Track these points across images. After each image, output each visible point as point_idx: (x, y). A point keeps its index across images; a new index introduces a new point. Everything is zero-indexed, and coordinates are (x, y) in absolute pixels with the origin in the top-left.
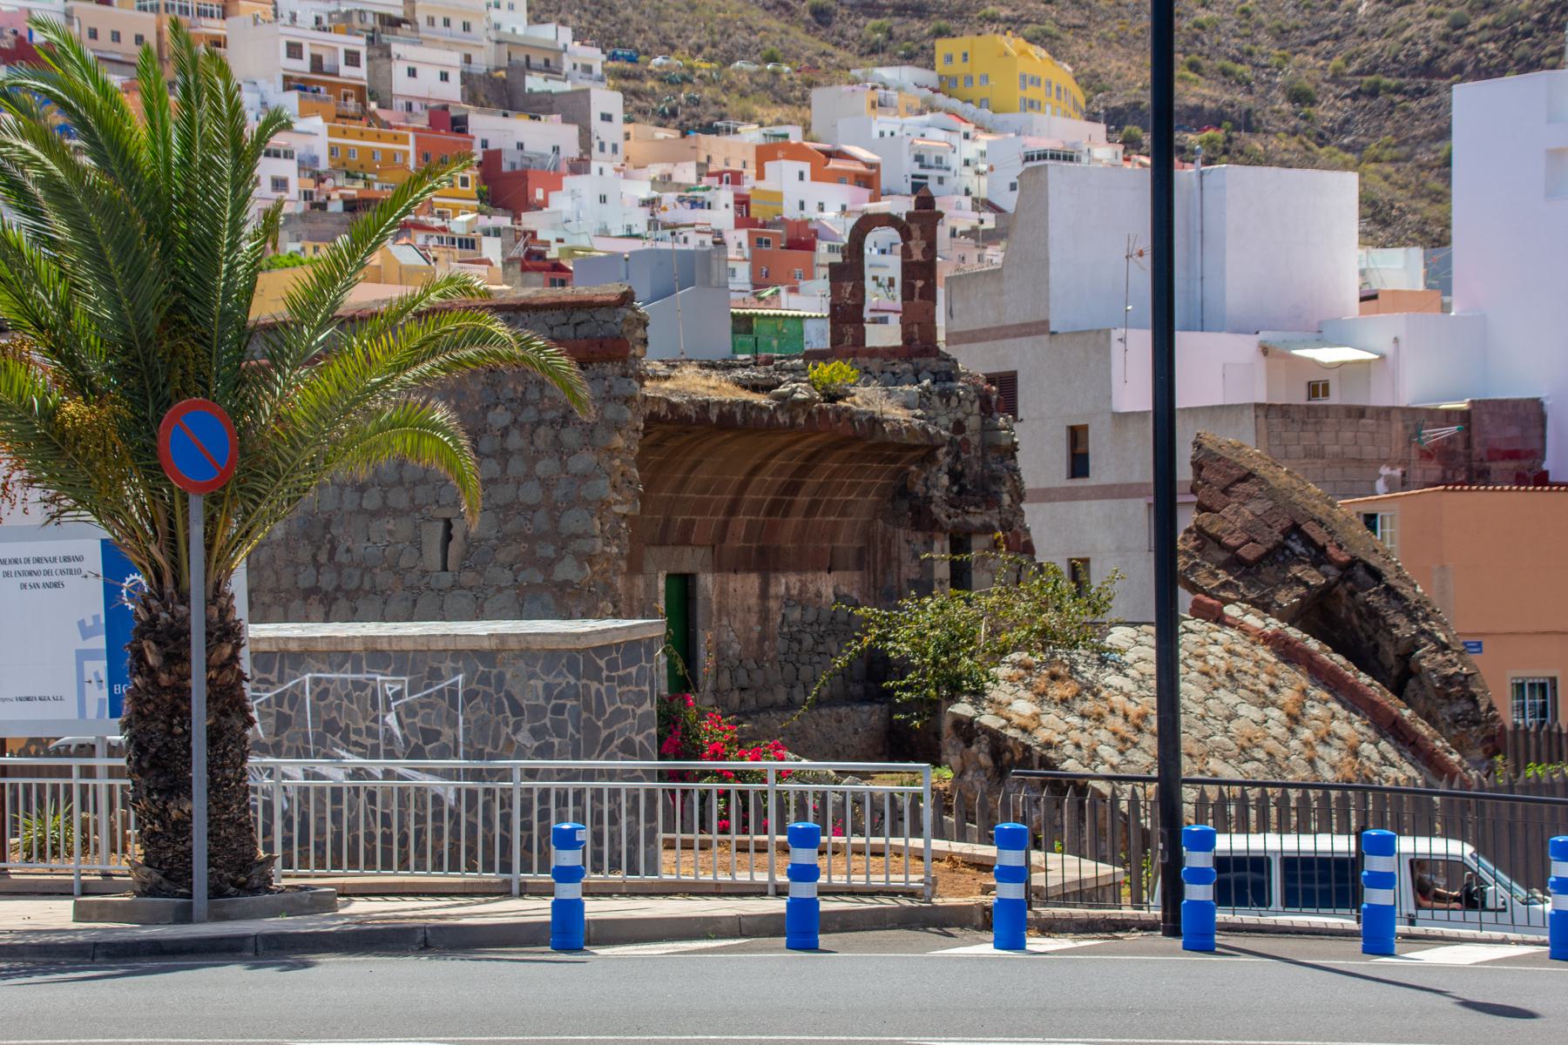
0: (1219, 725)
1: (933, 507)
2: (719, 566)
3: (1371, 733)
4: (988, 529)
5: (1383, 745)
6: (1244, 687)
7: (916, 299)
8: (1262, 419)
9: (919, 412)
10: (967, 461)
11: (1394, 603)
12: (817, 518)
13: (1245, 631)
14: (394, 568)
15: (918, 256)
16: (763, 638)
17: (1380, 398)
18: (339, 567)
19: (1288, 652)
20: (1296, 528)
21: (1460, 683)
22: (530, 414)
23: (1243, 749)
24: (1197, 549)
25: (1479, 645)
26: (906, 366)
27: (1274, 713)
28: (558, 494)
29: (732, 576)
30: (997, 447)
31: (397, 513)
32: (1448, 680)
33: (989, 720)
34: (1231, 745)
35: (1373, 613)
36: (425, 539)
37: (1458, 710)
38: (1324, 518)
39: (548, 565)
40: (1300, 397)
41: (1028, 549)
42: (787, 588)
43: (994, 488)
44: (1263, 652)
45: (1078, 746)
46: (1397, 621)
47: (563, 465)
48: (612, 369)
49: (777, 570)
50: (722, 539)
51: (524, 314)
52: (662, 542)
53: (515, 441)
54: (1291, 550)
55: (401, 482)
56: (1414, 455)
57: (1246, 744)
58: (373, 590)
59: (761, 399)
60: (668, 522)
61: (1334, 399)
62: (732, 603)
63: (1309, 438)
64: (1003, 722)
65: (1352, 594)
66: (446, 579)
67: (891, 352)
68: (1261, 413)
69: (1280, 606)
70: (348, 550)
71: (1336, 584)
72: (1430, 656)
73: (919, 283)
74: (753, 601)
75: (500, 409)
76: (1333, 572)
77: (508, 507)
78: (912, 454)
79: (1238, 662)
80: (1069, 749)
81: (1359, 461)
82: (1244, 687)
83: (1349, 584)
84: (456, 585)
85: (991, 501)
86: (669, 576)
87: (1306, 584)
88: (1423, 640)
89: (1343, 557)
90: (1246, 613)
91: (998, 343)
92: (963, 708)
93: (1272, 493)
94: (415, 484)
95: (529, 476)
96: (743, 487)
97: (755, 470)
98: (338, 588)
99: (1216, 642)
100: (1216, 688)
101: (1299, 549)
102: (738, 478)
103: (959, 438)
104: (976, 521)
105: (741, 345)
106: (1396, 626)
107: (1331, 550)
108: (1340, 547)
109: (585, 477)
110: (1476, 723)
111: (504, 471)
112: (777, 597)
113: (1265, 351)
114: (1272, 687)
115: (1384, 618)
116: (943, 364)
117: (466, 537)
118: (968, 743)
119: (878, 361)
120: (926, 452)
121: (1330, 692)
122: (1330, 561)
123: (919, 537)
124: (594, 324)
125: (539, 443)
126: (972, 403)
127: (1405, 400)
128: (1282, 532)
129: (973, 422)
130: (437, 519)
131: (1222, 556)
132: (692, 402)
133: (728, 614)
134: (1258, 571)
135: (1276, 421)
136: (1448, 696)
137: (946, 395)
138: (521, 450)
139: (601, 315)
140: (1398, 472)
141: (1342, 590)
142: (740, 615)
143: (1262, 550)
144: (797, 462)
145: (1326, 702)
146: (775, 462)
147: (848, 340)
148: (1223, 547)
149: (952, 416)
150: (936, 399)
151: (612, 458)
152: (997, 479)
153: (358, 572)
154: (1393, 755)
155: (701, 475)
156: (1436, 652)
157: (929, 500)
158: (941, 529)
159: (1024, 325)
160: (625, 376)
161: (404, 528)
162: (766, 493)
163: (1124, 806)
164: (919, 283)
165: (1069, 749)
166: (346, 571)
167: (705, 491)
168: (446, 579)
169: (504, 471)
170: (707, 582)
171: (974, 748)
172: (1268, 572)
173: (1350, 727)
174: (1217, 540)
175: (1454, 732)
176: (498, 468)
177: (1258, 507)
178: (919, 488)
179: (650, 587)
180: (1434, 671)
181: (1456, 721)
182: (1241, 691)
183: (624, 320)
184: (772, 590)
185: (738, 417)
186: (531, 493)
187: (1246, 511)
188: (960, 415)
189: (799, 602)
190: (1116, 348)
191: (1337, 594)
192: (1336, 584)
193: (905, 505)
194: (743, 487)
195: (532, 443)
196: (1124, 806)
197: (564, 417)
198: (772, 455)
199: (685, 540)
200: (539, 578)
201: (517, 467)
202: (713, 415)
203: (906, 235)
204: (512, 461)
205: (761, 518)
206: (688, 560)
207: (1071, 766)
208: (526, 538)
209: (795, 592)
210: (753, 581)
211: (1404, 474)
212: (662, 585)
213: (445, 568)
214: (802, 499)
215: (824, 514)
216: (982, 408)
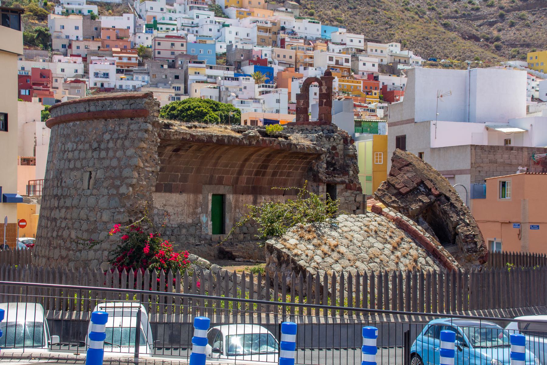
0: (365, 250)
1: (320, 175)
2: (236, 191)
3: (424, 254)
4: (342, 182)
5: (428, 259)
6: (380, 237)
7: (323, 106)
8: (473, 150)
9: (315, 142)
10: (338, 160)
11: (453, 209)
12: (277, 177)
13: (387, 216)
14: (76, 189)
15: (324, 91)
17: (526, 144)
18: (62, 187)
19: (400, 225)
20: (422, 182)
21: (471, 238)
22: (116, 136)
23: (371, 258)
24: (386, 189)
25: (538, 226)
26: (319, 128)
27: (388, 246)
28: (122, 163)
29: (241, 196)
30: (349, 156)
31: (78, 169)
32: (467, 236)
33: (279, 246)
34: (367, 256)
35: (445, 213)
36: (84, 178)
37: (469, 247)
38: (433, 179)
39: (118, 188)
40: (502, 144)
41: (360, 189)
43: (347, 169)
44: (392, 225)
45: (307, 256)
46: (453, 215)
47: (125, 153)
48: (141, 120)
49: (261, 194)
50: (237, 183)
51: (115, 101)
52: (210, 183)
53: (111, 145)
54: (420, 190)
55: (79, 159)
56: (531, 163)
57: (373, 257)
58: (70, 196)
59: (238, 135)
60: (212, 177)
61: (512, 144)
62: (240, 205)
63: (491, 156)
64: (283, 246)
65: (439, 205)
66: (89, 192)
67: (315, 123)
68: (473, 148)
69: (412, 209)
70: (65, 182)
71: (434, 202)
72: (461, 228)
73: (325, 100)
76: (433, 197)
77: (108, 167)
78: (311, 157)
79: (381, 228)
80: (304, 257)
81: (510, 165)
82: (380, 237)
83: (438, 202)
84: (91, 194)
85: (346, 173)
86: (214, 195)
87: (422, 202)
88: (461, 222)
89: (437, 193)
90: (390, 211)
91: (401, 126)
92: (271, 242)
93: (416, 170)
94: (83, 159)
95: (114, 157)
96: (243, 166)
97: (246, 160)
98: (62, 195)
99: (376, 221)
100: (368, 237)
101: (422, 189)
102: (240, 163)
103: (334, 152)
104: (339, 180)
105: (358, 130)
106: (452, 217)
107: (433, 190)
108: (436, 189)
109: (130, 157)
110: (476, 252)
111: (107, 155)
113: (487, 129)
114: (391, 237)
115: (448, 214)
116: (331, 127)
117: (95, 178)
118: (271, 253)
119: (310, 126)
120: (318, 156)
121: (412, 239)
122: (432, 194)
123: (315, 184)
124: (136, 104)
125: (118, 145)
126: (340, 140)
127: (534, 145)
128: (417, 184)
129: (340, 147)
130: (87, 171)
131: (395, 192)
132: (205, 135)
133: (239, 208)
134: (407, 197)
135: (479, 151)
136: (466, 242)
137: (328, 138)
138: (112, 148)
139: (138, 101)
140: (525, 169)
141: (436, 204)
143: (408, 189)
144: (263, 158)
145: (410, 242)
146: (254, 157)
147: (302, 119)
148: (396, 188)
149: (331, 144)
150: (324, 139)
151: (142, 151)
152: (348, 166)
154: (431, 262)
155: (223, 161)
156: (464, 226)
157: (318, 172)
158: (322, 182)
159: (408, 120)
160: (146, 122)
162: (253, 168)
163: (322, 279)
164: (325, 100)
165: (304, 257)
166: (64, 189)
167: (227, 167)
168: (89, 192)
169: (107, 155)
170: (230, 198)
171: (273, 255)
172: (410, 197)
173: (415, 251)
174: (393, 186)
175: (467, 255)
176: (105, 154)
177: (410, 175)
178: (315, 168)
179: (205, 198)
180: (462, 233)
181: (468, 251)
182: (378, 238)
183: (145, 103)
184: (259, 201)
185: (226, 141)
186: (114, 163)
187: (405, 176)
188: (335, 144)
190: (432, 127)
191: (435, 206)
192: (434, 202)
193: (311, 174)
194: (243, 166)
195: (116, 145)
196: (322, 279)
197: (126, 136)
198: (252, 155)
199: (220, 182)
200: (115, 192)
201: (111, 153)
202: (215, 140)
203: (321, 85)
204: (110, 152)
205: (253, 176)
207: (302, 263)
208: (112, 178)
210: (251, 198)
211: (527, 169)
212: (210, 197)
213: (89, 189)
214: (270, 170)
215: (280, 176)
216: (344, 142)
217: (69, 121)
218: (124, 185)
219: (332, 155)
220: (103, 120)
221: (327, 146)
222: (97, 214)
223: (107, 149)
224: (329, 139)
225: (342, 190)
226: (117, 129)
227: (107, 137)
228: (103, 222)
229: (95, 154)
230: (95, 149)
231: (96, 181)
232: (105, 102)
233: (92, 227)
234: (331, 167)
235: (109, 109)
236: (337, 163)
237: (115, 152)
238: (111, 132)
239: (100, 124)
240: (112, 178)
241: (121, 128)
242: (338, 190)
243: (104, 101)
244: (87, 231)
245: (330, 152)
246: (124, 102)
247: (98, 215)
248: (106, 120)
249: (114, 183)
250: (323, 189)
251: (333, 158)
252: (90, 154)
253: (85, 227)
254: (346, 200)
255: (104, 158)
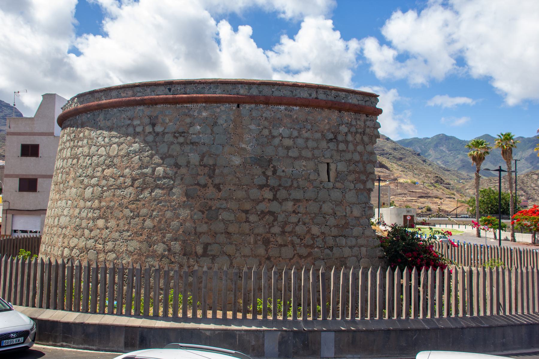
14: (308, 179)
31: (307, 159)
36: (320, 169)
47: (365, 148)
51: (351, 94)
58: (298, 187)
66: (331, 185)
75: (344, 126)
77: (350, 161)
95: (355, 150)
98: (280, 185)
111: (347, 148)
130: (325, 163)
153: (290, 180)
161: (311, 164)
169: (347, 148)
186: (357, 157)
201: (351, 147)
213: (329, 181)
217: (307, 106)
218: (370, 181)
220: (337, 112)
222: (346, 209)
223: (347, 142)
226: (354, 123)
227: (344, 129)
228: (355, 217)
229: (332, 145)
230: (331, 140)
231: (338, 173)
232: (340, 93)
233: (343, 222)
235: (343, 101)
237: (356, 145)
238: (348, 125)
239: (334, 115)
240: (357, 172)
241: (358, 122)
243: (339, 92)
244: (337, 226)
246: (360, 97)
247: (347, 210)
248: (340, 112)
249: (360, 178)
252: (324, 144)
253: (332, 221)
255: (343, 151)
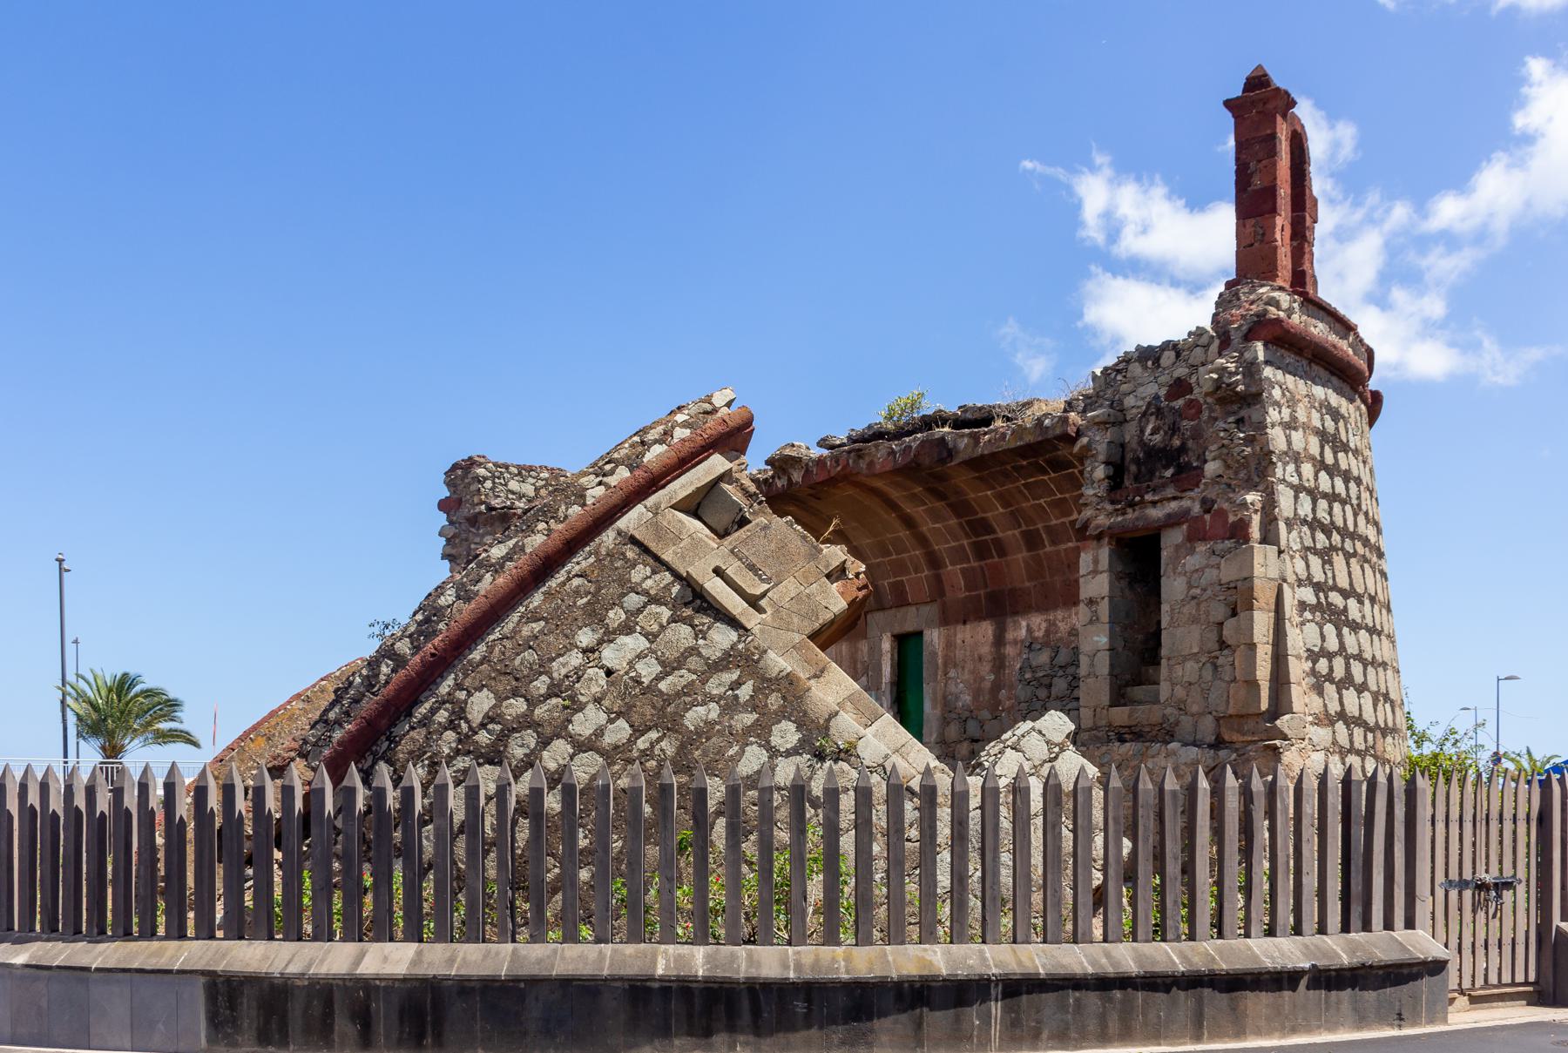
2: (946, 620)
4: (1173, 521)
12: (1048, 549)
16: (996, 687)
29: (960, 627)
42: (1029, 630)
49: (1015, 613)
50: (942, 593)
62: (959, 654)
74: (986, 650)
103: (1179, 403)
112: (1015, 642)
133: (955, 666)
142: (969, 666)
149: (1163, 379)
170: (934, 638)
184: (1010, 636)
188: (1181, 371)
189: (1046, 644)
199: (901, 601)
206: (909, 620)
209: (1039, 634)
210: (986, 629)
212: (886, 645)
219: (1169, 419)
221: (1151, 389)
224: (1157, 361)
225: (1178, 547)
234: (1166, 467)
236: (1190, 443)
242: (1164, 554)
245: (1159, 413)
250: (1096, 561)
251: (1174, 429)
254: (1190, 587)
